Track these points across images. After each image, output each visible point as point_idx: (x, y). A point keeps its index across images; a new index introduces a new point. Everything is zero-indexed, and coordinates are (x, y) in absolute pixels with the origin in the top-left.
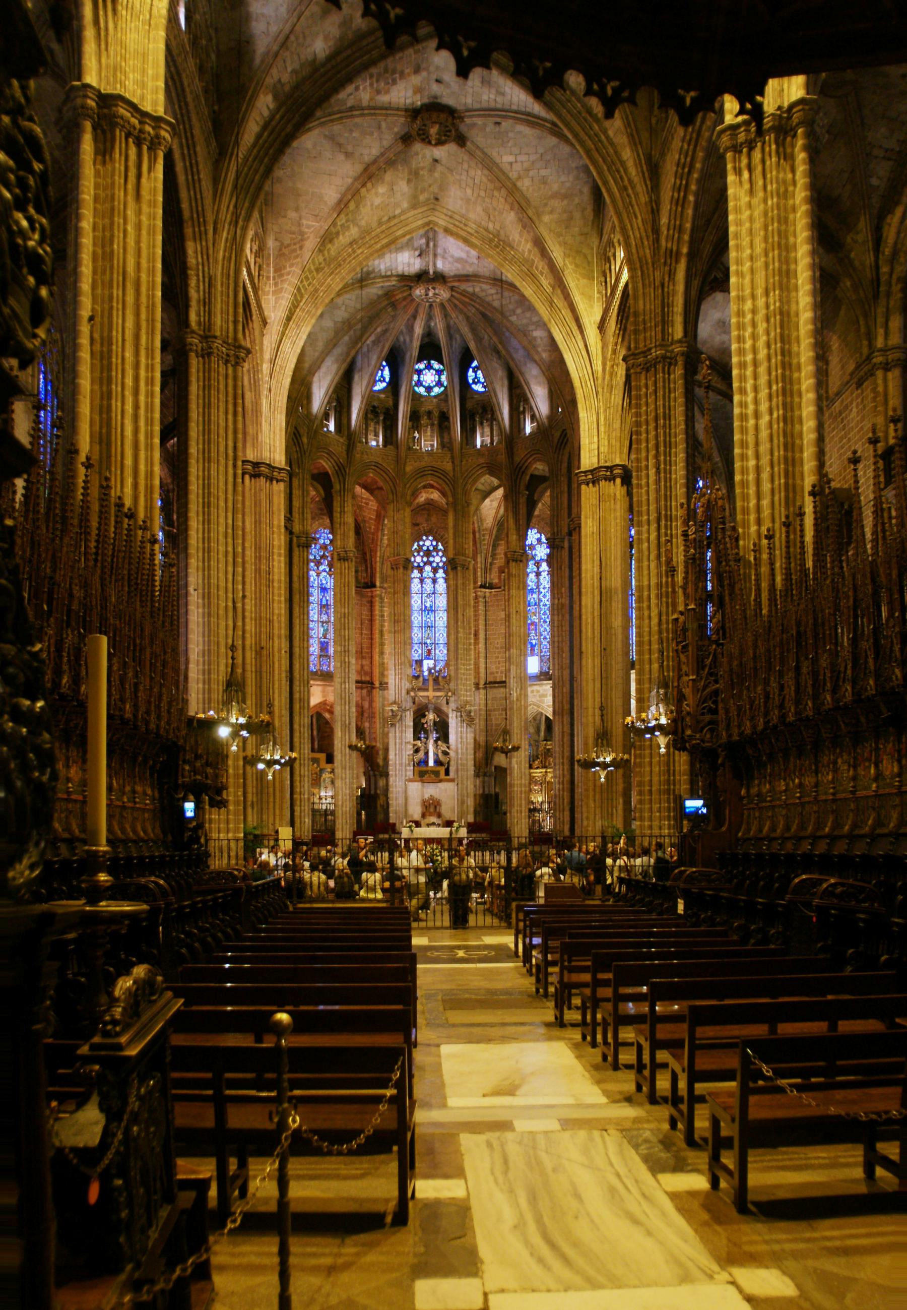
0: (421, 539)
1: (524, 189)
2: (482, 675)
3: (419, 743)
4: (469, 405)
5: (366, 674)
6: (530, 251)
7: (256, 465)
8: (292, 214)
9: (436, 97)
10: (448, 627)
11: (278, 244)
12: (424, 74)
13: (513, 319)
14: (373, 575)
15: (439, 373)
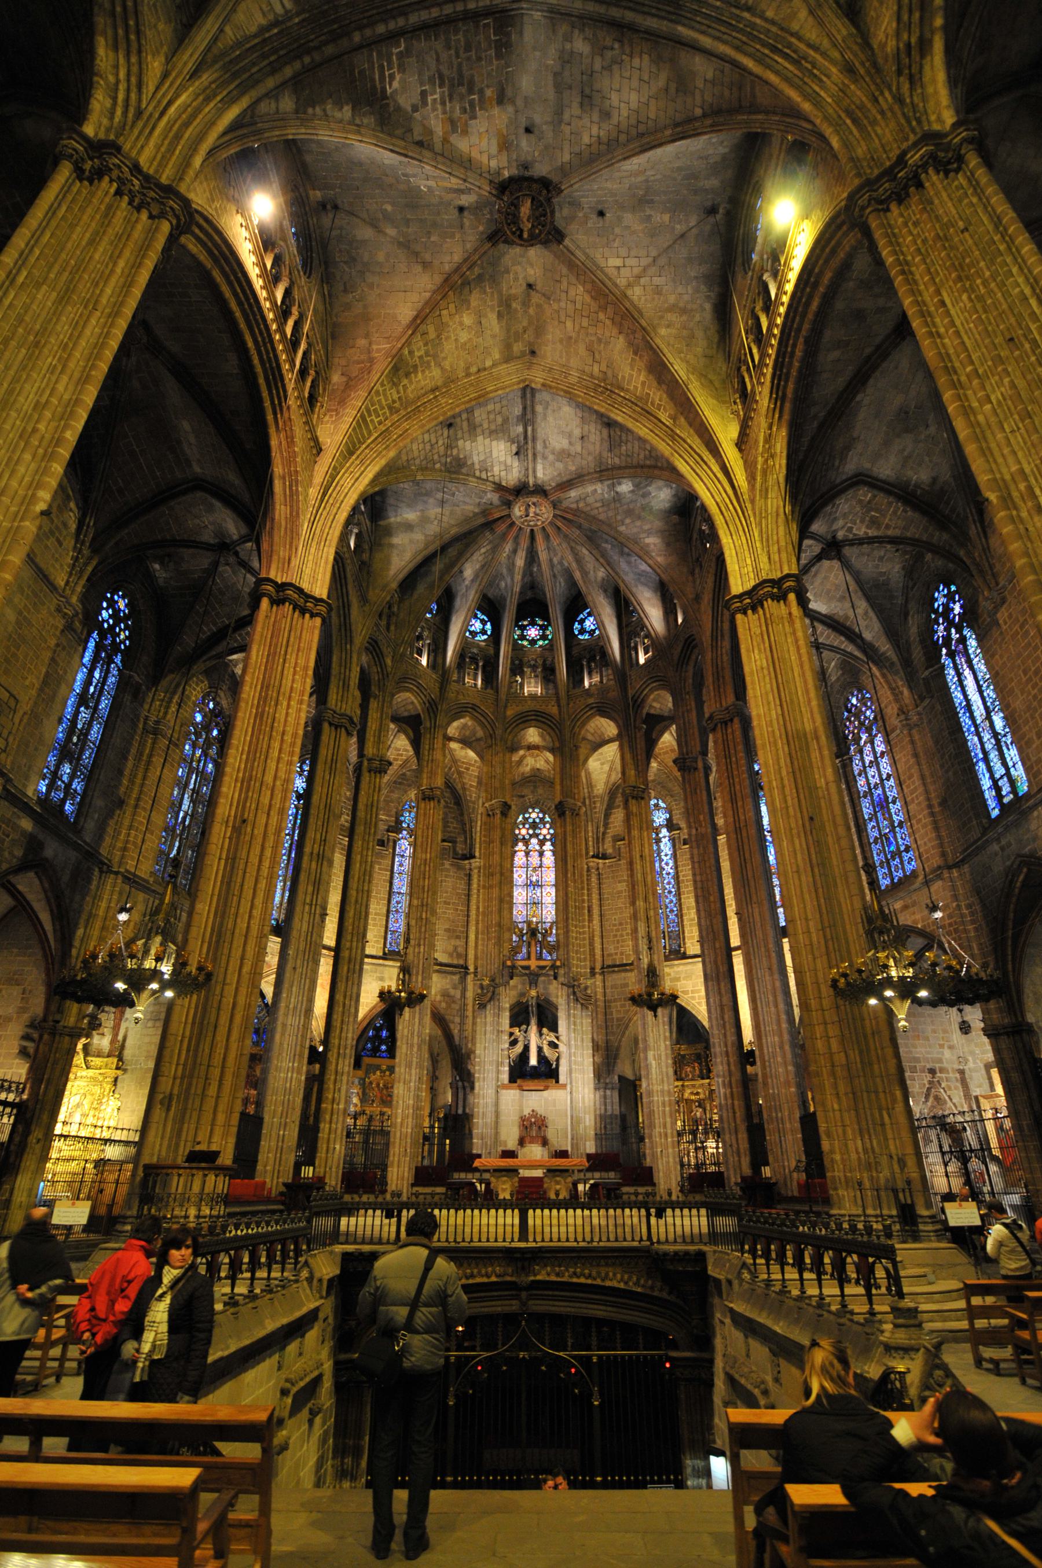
0: (526, 811)
1: (635, 298)
2: (598, 957)
3: (516, 1030)
4: (575, 651)
5: (459, 956)
6: (643, 383)
7: (282, 587)
8: (362, 342)
9: (526, 167)
10: (556, 903)
11: (345, 379)
12: (510, 109)
13: (622, 528)
14: (472, 847)
15: (543, 628)
